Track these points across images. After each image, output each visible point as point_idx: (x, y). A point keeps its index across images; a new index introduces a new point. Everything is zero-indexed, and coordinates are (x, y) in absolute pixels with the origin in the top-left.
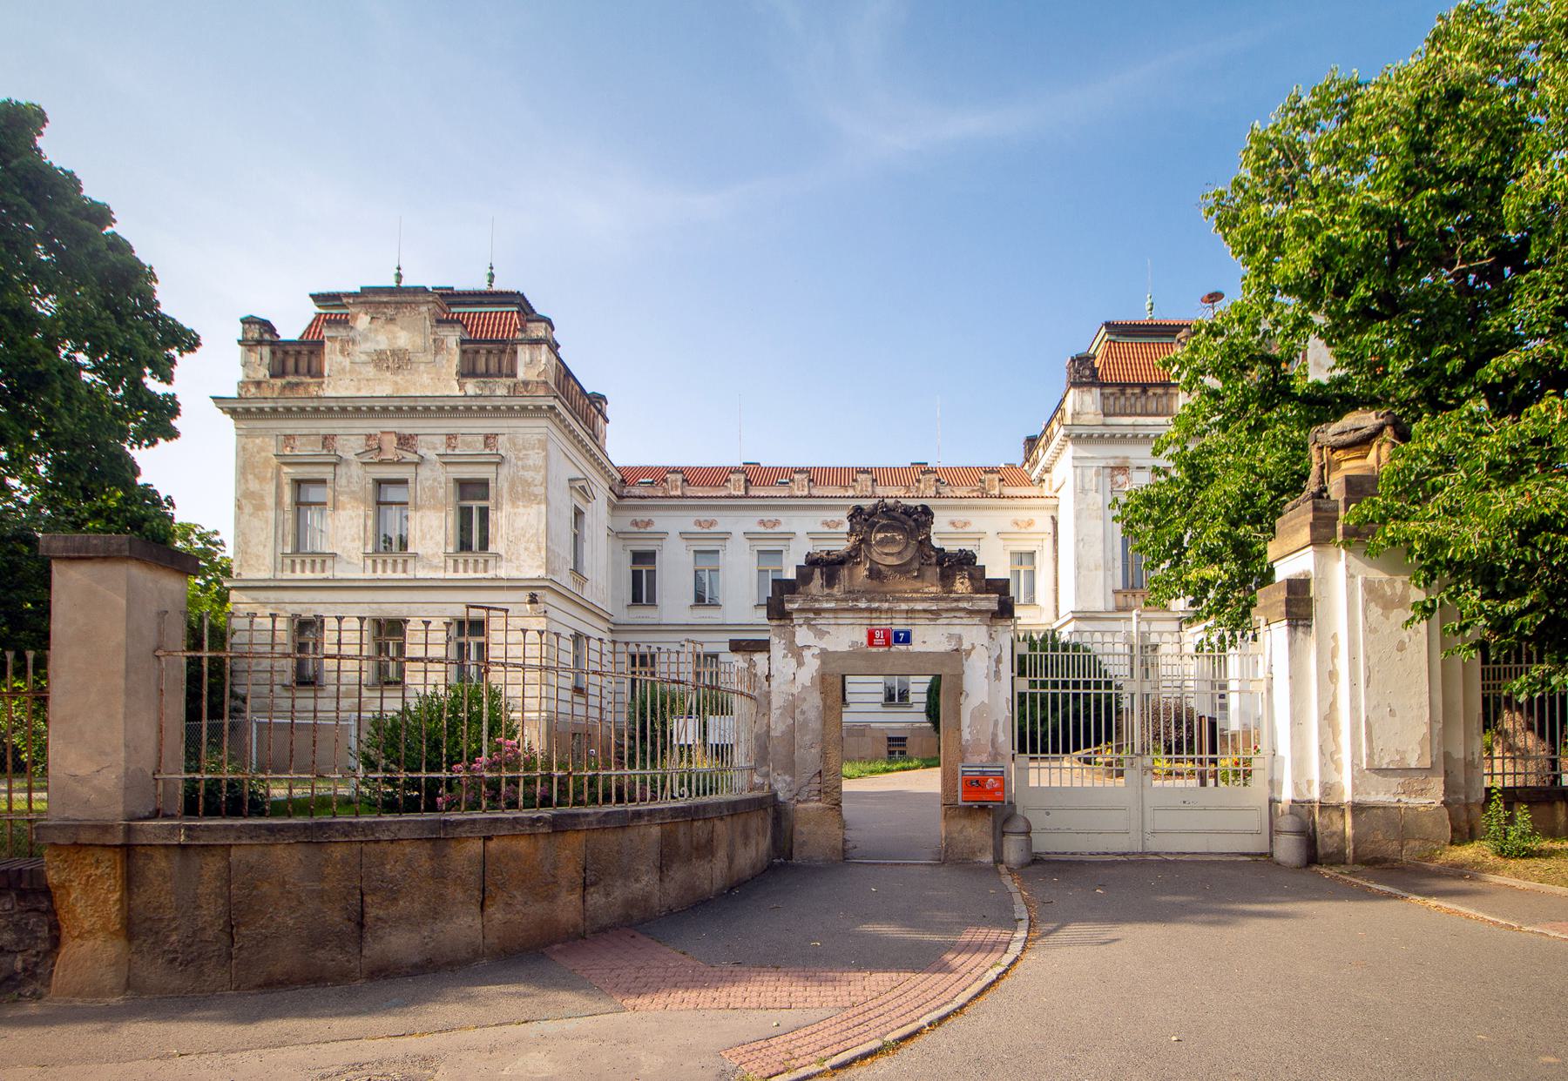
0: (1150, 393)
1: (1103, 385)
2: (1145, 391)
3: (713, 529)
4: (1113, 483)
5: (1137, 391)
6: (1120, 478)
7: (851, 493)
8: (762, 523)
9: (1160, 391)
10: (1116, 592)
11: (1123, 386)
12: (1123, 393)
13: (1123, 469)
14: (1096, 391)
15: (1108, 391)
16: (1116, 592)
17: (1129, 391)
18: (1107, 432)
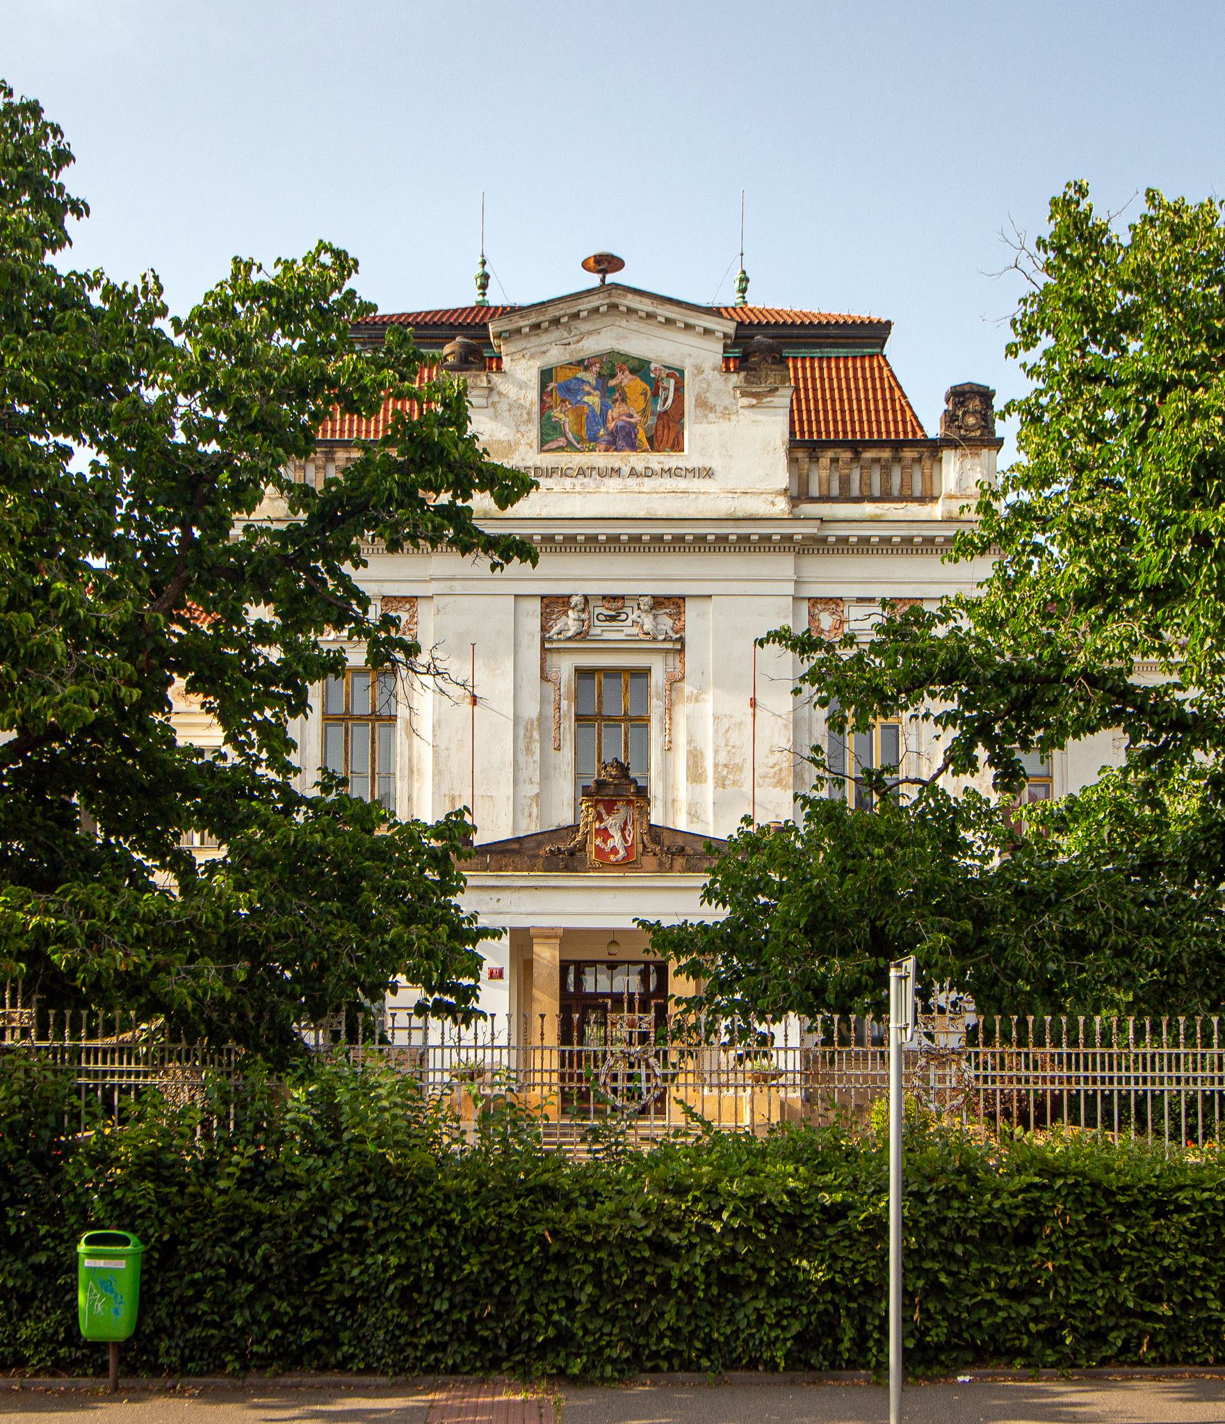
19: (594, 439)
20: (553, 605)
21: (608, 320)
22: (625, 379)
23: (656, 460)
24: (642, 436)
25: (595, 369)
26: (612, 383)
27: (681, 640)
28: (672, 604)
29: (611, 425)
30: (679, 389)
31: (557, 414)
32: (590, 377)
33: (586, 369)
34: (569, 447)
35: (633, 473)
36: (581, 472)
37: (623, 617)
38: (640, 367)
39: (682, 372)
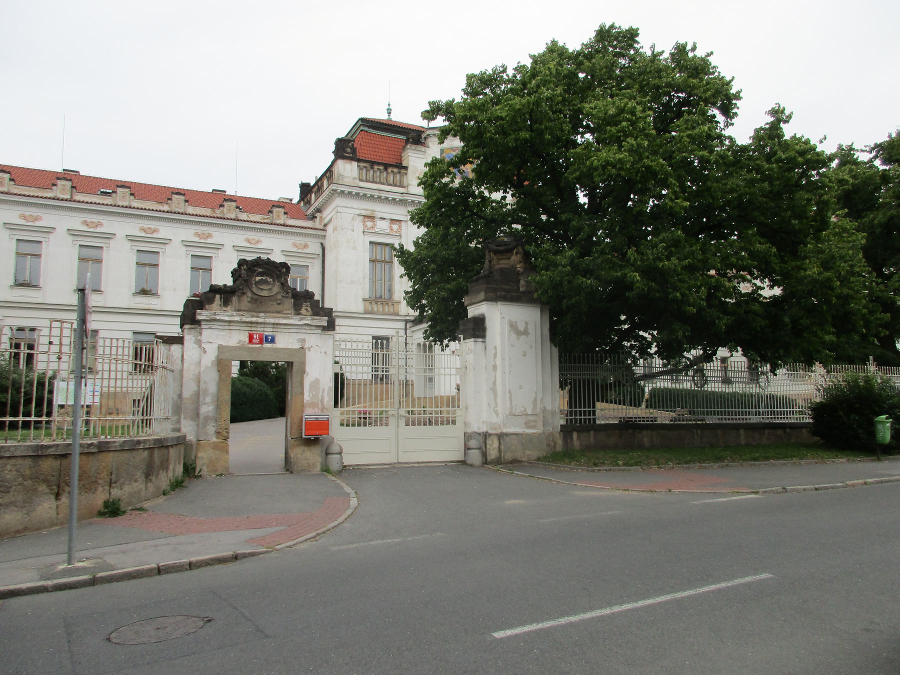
1: (359, 161)
2: (386, 169)
3: (37, 224)
4: (365, 226)
5: (381, 168)
6: (369, 224)
7: (166, 208)
8: (86, 223)
9: (396, 170)
10: (364, 300)
11: (372, 163)
12: (372, 168)
13: (372, 218)
14: (355, 164)
15: (362, 164)
16: (364, 300)
17: (376, 167)
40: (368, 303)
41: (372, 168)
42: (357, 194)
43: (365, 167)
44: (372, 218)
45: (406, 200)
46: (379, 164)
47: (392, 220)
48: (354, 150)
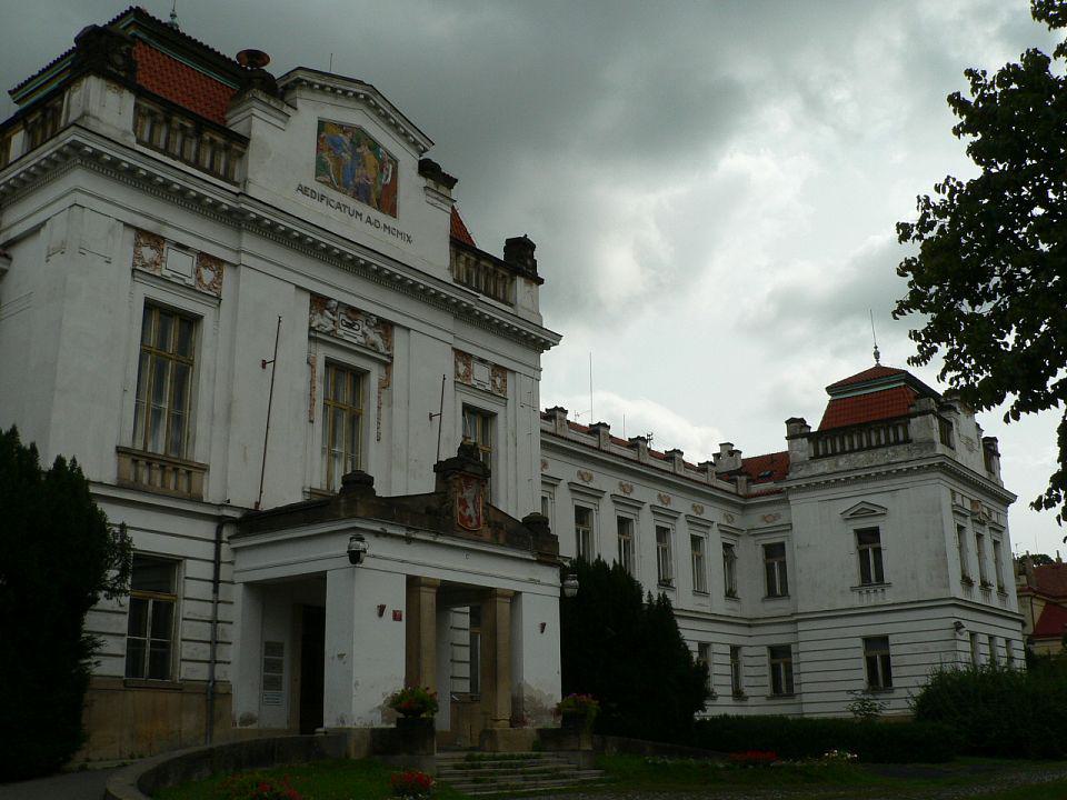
0: (207, 137)
2: (198, 133)
4: (138, 256)
6: (148, 253)
10: (120, 451)
12: (168, 121)
16: (120, 451)
17: (177, 120)
18: (145, 167)
19: (346, 185)
20: (319, 302)
21: (361, 106)
22: (364, 150)
23: (376, 214)
24: (373, 196)
25: (350, 135)
26: (358, 150)
27: (391, 357)
28: (386, 326)
29: (356, 180)
30: (395, 173)
31: (325, 155)
32: (346, 139)
33: (345, 132)
34: (329, 184)
35: (369, 220)
36: (339, 206)
37: (356, 327)
38: (375, 146)
39: (396, 162)
40: (127, 462)
41: (168, 121)
42: (132, 170)
43: (152, 114)
44: (156, 240)
45: (243, 213)
46: (185, 113)
47: (205, 259)
48: (131, 67)
